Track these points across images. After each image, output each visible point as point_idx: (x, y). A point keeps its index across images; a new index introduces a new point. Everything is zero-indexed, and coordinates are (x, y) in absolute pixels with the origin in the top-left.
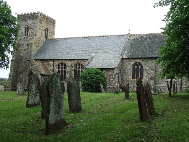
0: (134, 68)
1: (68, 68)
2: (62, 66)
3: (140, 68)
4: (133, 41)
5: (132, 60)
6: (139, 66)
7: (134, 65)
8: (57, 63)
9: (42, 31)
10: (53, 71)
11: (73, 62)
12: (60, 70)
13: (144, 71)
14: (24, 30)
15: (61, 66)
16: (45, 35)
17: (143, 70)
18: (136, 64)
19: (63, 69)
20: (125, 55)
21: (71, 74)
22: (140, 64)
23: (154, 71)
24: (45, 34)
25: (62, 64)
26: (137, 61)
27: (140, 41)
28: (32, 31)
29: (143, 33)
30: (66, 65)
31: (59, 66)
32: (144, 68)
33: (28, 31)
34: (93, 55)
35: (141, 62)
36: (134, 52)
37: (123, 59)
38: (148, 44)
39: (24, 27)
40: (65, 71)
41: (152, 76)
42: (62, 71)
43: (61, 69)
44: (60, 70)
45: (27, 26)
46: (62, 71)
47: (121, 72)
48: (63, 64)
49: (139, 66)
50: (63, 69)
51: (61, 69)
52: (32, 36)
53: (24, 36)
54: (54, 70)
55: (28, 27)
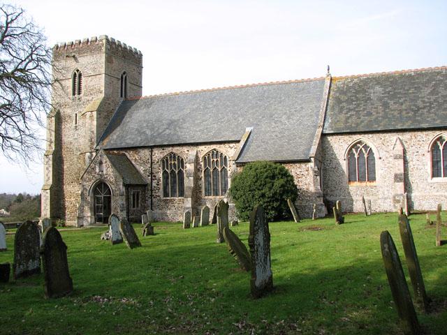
0: (350, 153)
1: (188, 165)
2: (173, 162)
3: (366, 156)
4: (341, 91)
5: (346, 137)
6: (364, 152)
7: (351, 149)
8: (158, 154)
9: (115, 81)
10: (152, 173)
11: (201, 148)
12: (169, 171)
13: (377, 162)
14: (71, 80)
15: (171, 160)
16: (122, 90)
17: (374, 159)
18: (355, 146)
19: (175, 168)
20: (327, 125)
21: (197, 179)
22: (366, 147)
23: (401, 161)
24: (122, 84)
25: (173, 156)
26: (356, 138)
27: (357, 92)
28: (91, 84)
29: (362, 74)
30: (182, 159)
31: (164, 161)
32: (376, 156)
33: (80, 83)
34: (248, 130)
35: (366, 139)
36: (348, 118)
37: (324, 135)
38: (380, 99)
39: (70, 75)
40: (181, 173)
41: (398, 172)
42: (172, 172)
43: (171, 168)
44: (169, 171)
45: (78, 71)
46: (172, 172)
47: (322, 168)
48: (174, 157)
49: (354, 152)
50: (175, 168)
51: (171, 168)
52: (91, 94)
53: (71, 96)
54: (154, 171)
55: (80, 75)
